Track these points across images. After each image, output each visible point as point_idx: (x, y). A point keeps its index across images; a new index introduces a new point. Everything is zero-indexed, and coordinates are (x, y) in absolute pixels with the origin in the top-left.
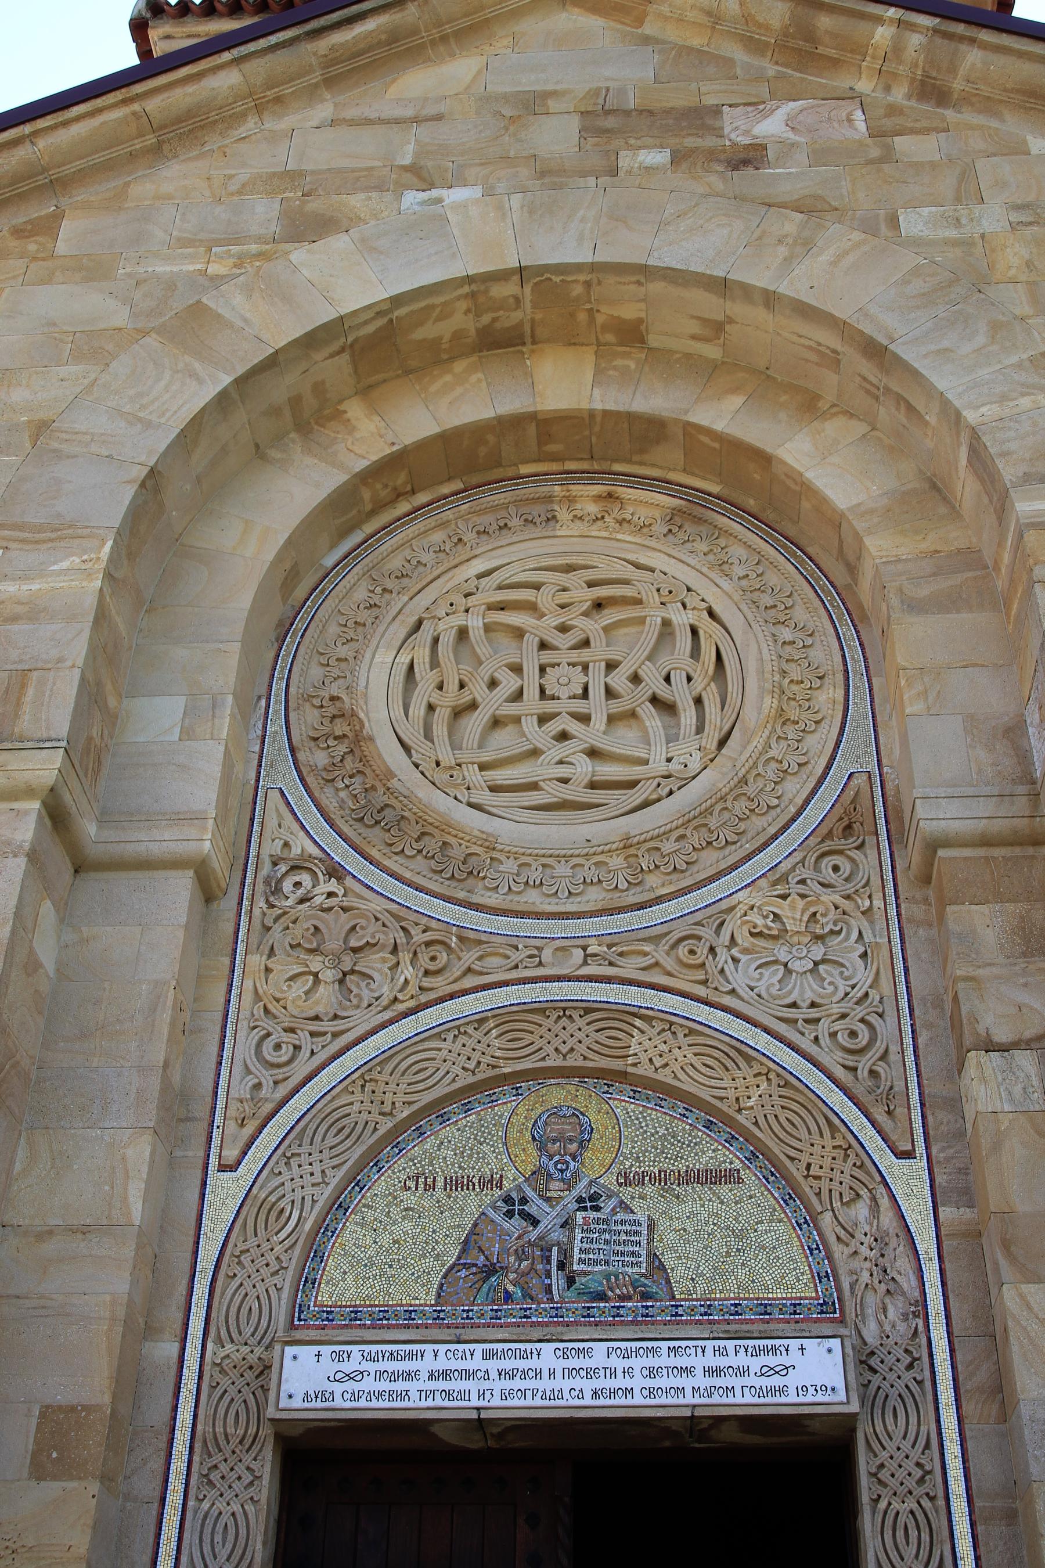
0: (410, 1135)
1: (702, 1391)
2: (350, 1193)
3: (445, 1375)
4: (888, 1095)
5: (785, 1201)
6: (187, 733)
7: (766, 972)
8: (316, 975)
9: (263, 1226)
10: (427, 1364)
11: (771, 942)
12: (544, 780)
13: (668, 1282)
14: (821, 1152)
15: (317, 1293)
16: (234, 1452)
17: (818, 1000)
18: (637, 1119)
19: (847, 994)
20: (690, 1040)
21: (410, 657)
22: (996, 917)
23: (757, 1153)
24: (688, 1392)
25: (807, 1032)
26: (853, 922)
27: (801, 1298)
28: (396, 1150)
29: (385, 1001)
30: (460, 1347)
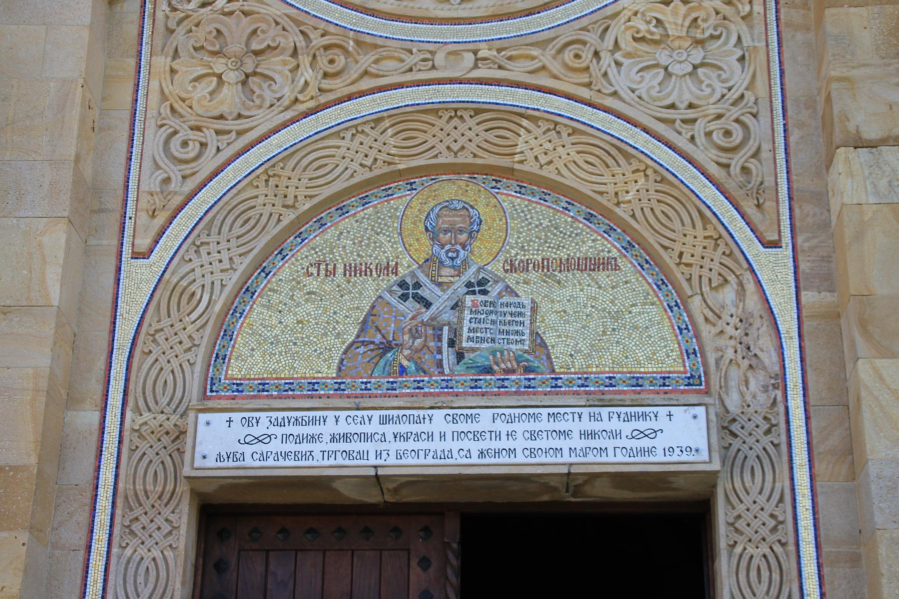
0: (312, 226)
1: (578, 451)
2: (256, 278)
3: (346, 437)
4: (758, 190)
5: (658, 286)
7: (648, 75)
8: (219, 77)
9: (176, 308)
10: (329, 428)
11: (653, 46)
13: (549, 357)
14: (693, 242)
15: (228, 368)
16: (153, 506)
17: (695, 102)
18: (523, 212)
19: (723, 96)
20: (574, 139)
22: (874, 19)
23: (633, 243)
24: (566, 452)
25: (684, 131)
26: (732, 27)
27: (670, 372)
28: (299, 240)
29: (286, 102)
30: (360, 413)
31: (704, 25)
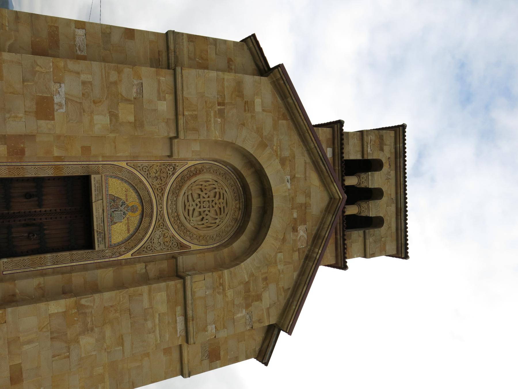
23: (132, 236)
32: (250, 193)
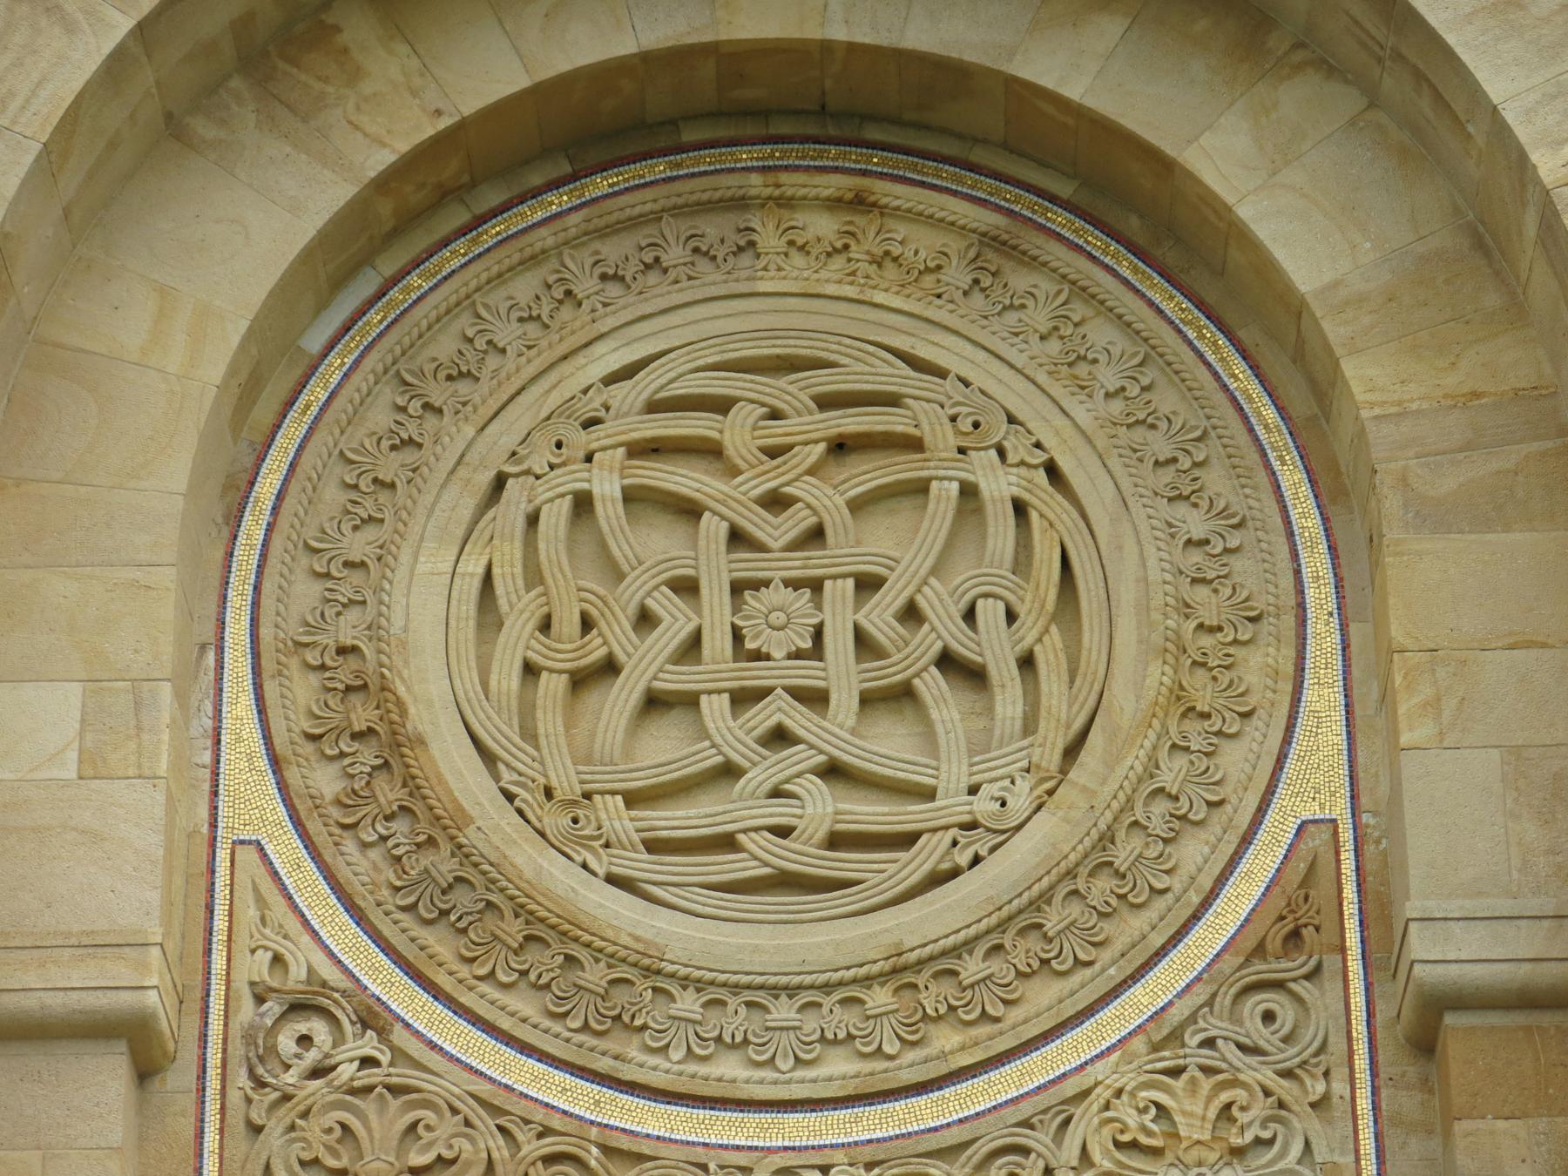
6: (92, 767)
12: (745, 831)
21: (484, 562)
22: (1539, 1144)
31: (1243, 1118)
32: (648, 60)
